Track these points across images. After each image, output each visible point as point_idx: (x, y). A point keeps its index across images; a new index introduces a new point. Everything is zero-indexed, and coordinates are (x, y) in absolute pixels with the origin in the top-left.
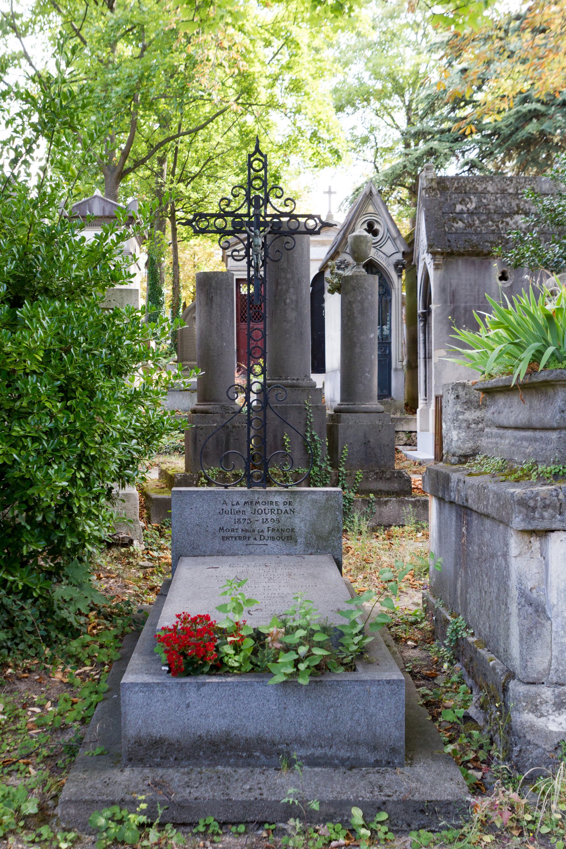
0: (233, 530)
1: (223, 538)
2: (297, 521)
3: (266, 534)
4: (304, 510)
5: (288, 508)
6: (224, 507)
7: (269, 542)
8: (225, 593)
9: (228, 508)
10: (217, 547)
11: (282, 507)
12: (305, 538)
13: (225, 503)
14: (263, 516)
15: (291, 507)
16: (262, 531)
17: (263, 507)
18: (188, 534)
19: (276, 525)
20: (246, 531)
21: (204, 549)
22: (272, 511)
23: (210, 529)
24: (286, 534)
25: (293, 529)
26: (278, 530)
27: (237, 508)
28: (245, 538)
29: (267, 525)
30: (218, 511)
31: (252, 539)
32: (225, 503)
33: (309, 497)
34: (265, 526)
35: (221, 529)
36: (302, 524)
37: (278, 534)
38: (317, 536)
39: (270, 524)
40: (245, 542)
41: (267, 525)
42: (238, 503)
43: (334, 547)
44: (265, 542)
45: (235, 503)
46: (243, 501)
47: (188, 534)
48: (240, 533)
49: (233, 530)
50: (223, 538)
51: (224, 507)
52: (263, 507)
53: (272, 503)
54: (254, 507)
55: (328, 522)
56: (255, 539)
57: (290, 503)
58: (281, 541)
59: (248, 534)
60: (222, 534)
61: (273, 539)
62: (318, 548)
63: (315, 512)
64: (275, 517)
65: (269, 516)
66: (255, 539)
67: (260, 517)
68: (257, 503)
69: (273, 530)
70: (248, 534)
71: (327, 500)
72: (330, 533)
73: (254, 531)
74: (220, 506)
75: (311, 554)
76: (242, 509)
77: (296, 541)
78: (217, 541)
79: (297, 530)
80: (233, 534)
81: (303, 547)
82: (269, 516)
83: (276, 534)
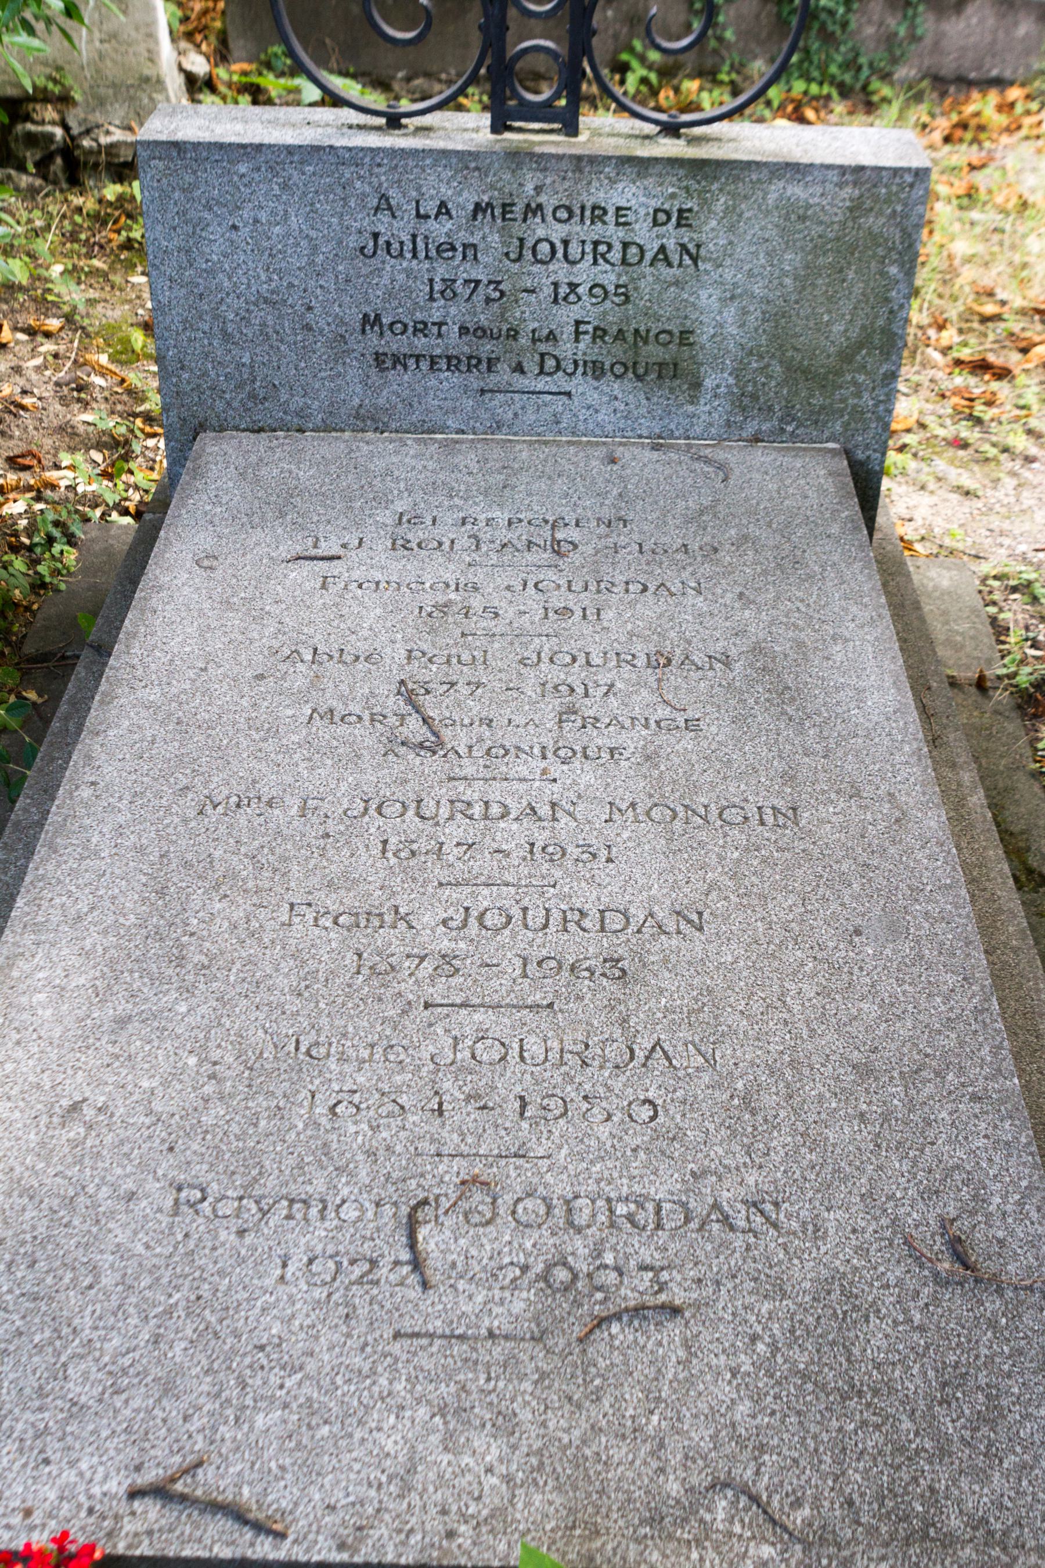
0: (421, 328)
1: (379, 358)
2: (708, 298)
3: (566, 349)
4: (742, 251)
5: (671, 237)
6: (383, 224)
7: (579, 385)
8: (153, 1447)
9: (400, 229)
10: (355, 395)
11: (643, 233)
12: (736, 373)
13: (384, 204)
14: (560, 270)
15: (686, 236)
16: (552, 337)
17: (557, 232)
18: (226, 336)
19: (612, 314)
20: (482, 332)
21: (298, 402)
22: (598, 251)
23: (318, 319)
24: (653, 352)
25: (685, 334)
26: (620, 335)
27: (439, 229)
28: (473, 362)
29: (575, 312)
30: (353, 242)
31: (503, 367)
32: (384, 204)
33: (775, 190)
34: (566, 315)
35: (371, 322)
36: (730, 314)
37: (618, 350)
38: (789, 368)
39: (585, 309)
40: (474, 381)
41: (575, 312)
42: (443, 209)
43: (857, 413)
44: (560, 381)
45: (430, 207)
46: (469, 198)
47: (226, 336)
48: (453, 341)
49: (421, 328)
50: (379, 358)
51: (383, 224)
52: (557, 232)
53: (598, 213)
54: (518, 229)
55: (846, 307)
56: (519, 369)
57: (683, 219)
58: (629, 382)
59: (487, 348)
60: (373, 341)
61: (596, 370)
62: (788, 416)
63: (791, 259)
64: (609, 278)
65: (585, 273)
66: (519, 369)
67: (543, 277)
68: (533, 210)
69: (599, 333)
70: (487, 348)
71: (856, 209)
72: (847, 356)
73: (513, 334)
74: (364, 221)
75: (756, 439)
76: (462, 237)
77: (697, 385)
78: (353, 371)
79: (704, 336)
80: (421, 343)
81: (722, 406)
82: (585, 273)
83: (609, 353)
